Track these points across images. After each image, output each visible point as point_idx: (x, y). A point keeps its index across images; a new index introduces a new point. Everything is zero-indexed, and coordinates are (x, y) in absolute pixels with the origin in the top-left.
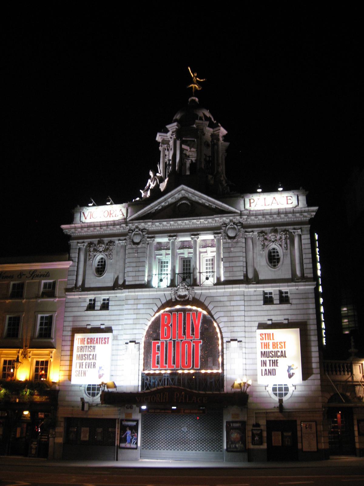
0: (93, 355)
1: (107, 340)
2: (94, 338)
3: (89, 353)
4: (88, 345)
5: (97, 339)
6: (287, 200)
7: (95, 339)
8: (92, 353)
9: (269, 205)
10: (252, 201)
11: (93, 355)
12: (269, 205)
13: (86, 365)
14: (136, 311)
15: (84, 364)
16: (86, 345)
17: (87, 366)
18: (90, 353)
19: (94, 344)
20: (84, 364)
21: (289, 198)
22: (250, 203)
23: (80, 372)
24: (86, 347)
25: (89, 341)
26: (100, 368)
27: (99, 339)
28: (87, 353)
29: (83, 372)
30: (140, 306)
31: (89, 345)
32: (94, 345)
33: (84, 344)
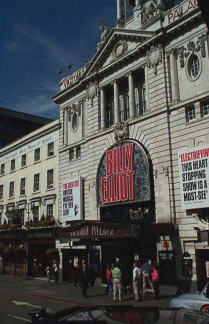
9: (185, 12)
10: (170, 16)
12: (185, 12)
22: (169, 19)
26: (76, 206)
30: (96, 149)
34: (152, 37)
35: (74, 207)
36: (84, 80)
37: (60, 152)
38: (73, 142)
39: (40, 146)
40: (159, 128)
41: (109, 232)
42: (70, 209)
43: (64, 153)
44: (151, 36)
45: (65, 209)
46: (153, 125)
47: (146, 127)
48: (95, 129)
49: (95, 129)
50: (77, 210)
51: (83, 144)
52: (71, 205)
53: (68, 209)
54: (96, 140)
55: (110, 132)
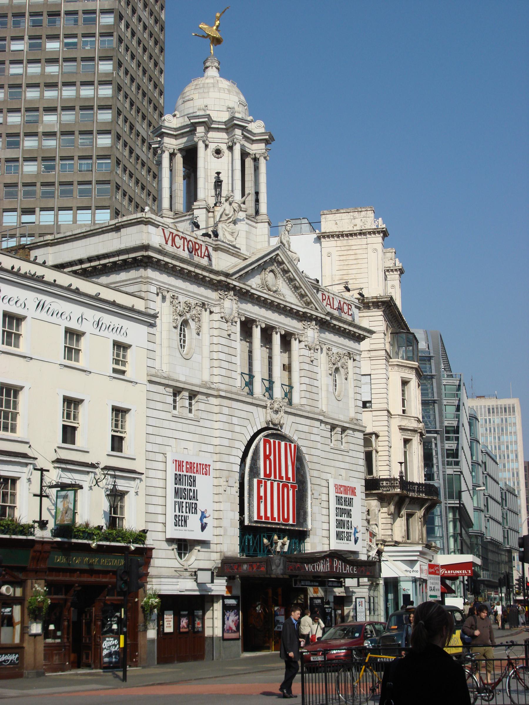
0: (194, 490)
1: (208, 469)
2: (194, 463)
3: (189, 488)
4: (187, 474)
5: (197, 464)
6: (349, 309)
7: (195, 465)
8: (192, 488)
11: (194, 490)
13: (186, 507)
14: (231, 427)
15: (184, 505)
16: (185, 473)
17: (188, 511)
18: (190, 488)
19: (194, 473)
20: (184, 505)
21: (350, 307)
23: (180, 518)
24: (185, 476)
25: (188, 466)
27: (199, 466)
28: (186, 487)
29: (183, 518)
30: (235, 420)
31: (189, 474)
32: (194, 475)
33: (183, 471)
34: (321, 313)
35: (199, 514)
36: (229, 281)
37: (150, 382)
38: (182, 379)
39: (85, 327)
40: (313, 437)
41: (353, 570)
42: (191, 515)
43: (161, 389)
44: (320, 310)
45: (177, 513)
46: (306, 429)
47: (300, 427)
48: (231, 382)
49: (231, 382)
50: (205, 520)
51: (208, 395)
52: (193, 508)
53: (184, 514)
54: (235, 404)
55: (257, 405)
